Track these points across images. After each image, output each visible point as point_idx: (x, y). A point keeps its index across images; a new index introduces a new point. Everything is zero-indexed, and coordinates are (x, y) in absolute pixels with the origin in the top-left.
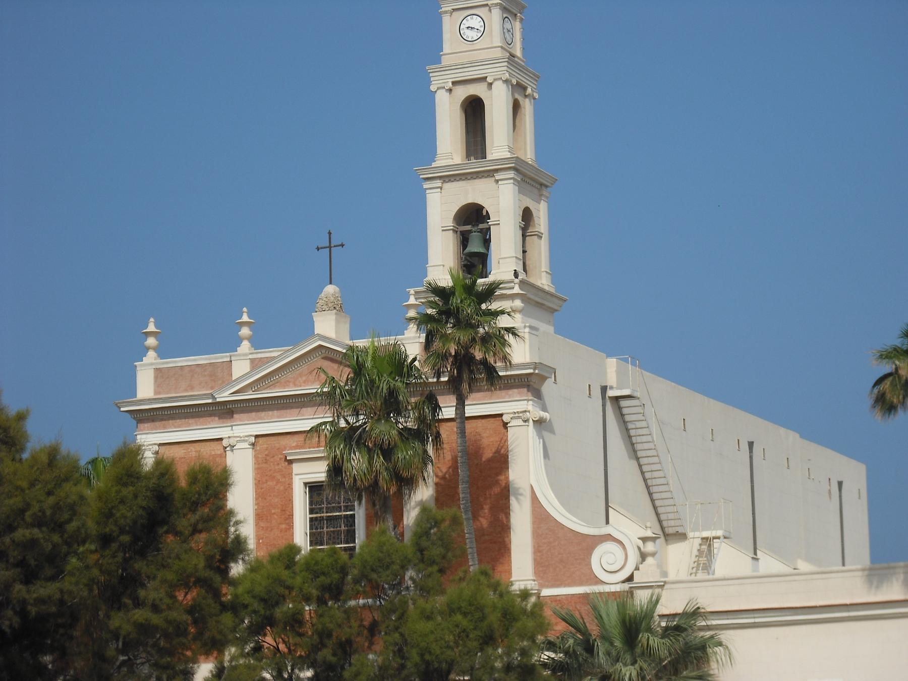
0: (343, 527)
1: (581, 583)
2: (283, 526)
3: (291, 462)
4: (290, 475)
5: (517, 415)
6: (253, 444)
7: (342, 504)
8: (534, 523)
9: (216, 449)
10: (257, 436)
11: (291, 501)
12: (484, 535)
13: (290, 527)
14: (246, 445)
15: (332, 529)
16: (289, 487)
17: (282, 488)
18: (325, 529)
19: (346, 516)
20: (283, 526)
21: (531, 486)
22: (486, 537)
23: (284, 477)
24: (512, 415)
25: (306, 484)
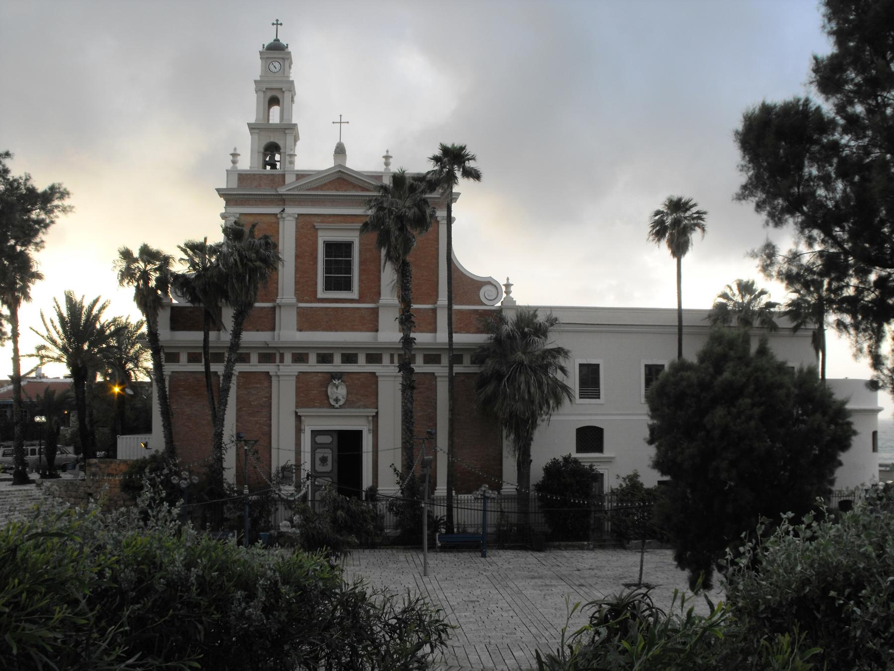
0: (343, 266)
1: (474, 304)
3: (317, 229)
6: (297, 219)
10: (298, 214)
11: (316, 250)
13: (316, 263)
16: (316, 242)
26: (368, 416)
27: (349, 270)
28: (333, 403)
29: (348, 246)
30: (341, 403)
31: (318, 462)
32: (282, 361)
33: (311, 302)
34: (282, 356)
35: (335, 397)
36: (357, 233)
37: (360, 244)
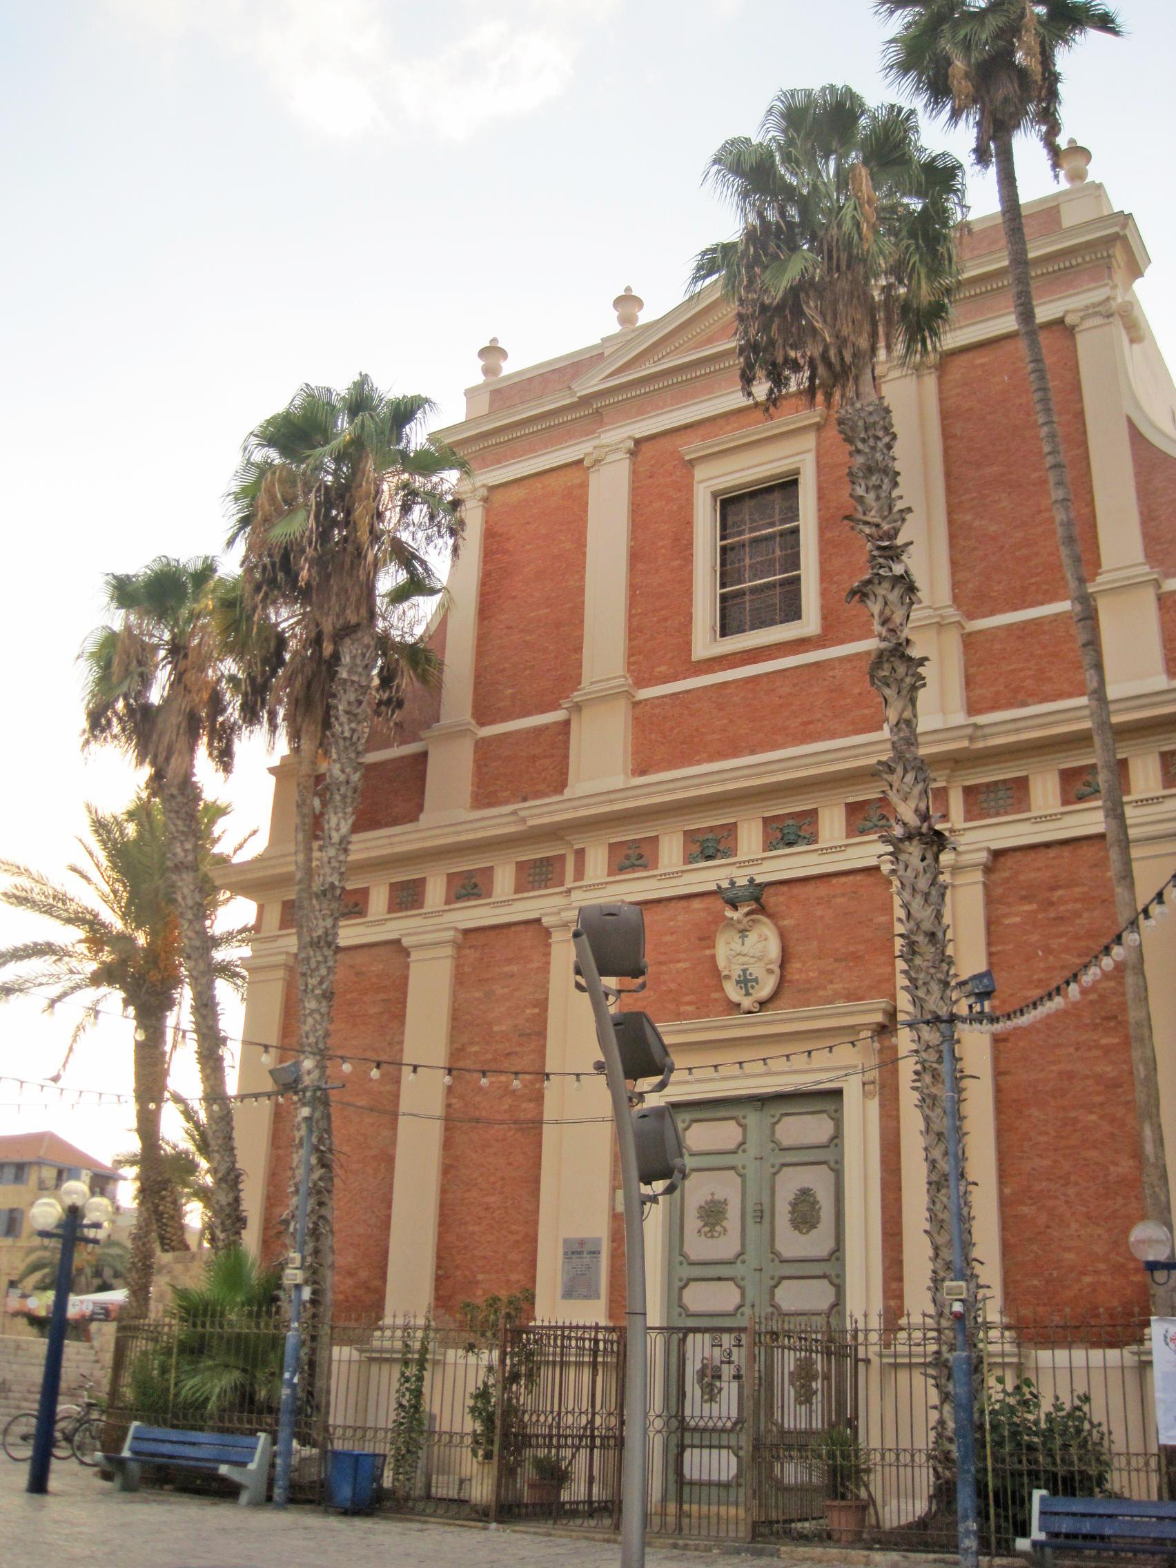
0: (778, 552)
2: (676, 563)
3: (691, 463)
4: (689, 488)
5: (1091, 311)
7: (777, 517)
8: (1137, 475)
9: (574, 477)
12: (1040, 512)
13: (688, 560)
14: (621, 455)
15: (759, 559)
16: (689, 503)
17: (675, 507)
18: (747, 561)
19: (782, 534)
20: (676, 563)
21: (1129, 420)
22: (1046, 515)
23: (680, 490)
24: (1082, 314)
25: (715, 495)
26: (854, 1029)
27: (793, 561)
28: (733, 992)
29: (788, 485)
30: (765, 991)
31: (693, 1223)
32: (580, 873)
33: (675, 678)
34: (580, 854)
35: (736, 972)
36: (809, 441)
37: (820, 468)
